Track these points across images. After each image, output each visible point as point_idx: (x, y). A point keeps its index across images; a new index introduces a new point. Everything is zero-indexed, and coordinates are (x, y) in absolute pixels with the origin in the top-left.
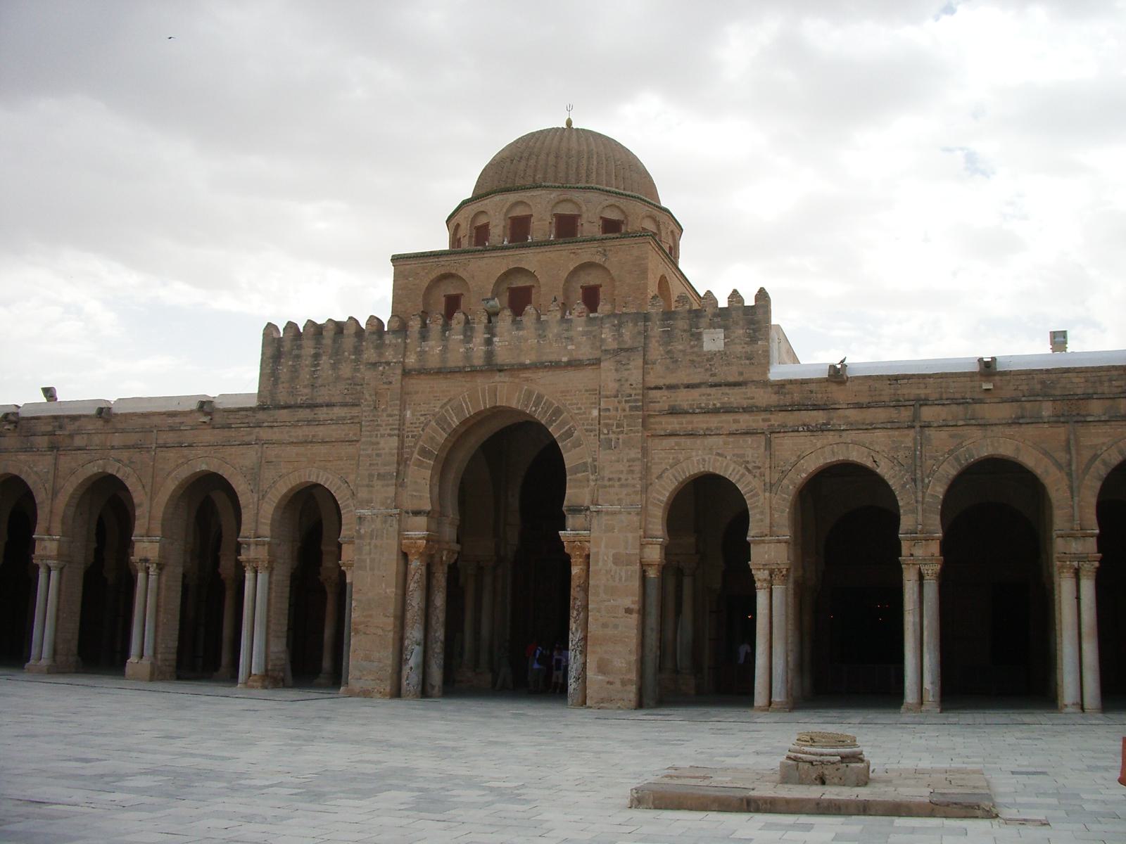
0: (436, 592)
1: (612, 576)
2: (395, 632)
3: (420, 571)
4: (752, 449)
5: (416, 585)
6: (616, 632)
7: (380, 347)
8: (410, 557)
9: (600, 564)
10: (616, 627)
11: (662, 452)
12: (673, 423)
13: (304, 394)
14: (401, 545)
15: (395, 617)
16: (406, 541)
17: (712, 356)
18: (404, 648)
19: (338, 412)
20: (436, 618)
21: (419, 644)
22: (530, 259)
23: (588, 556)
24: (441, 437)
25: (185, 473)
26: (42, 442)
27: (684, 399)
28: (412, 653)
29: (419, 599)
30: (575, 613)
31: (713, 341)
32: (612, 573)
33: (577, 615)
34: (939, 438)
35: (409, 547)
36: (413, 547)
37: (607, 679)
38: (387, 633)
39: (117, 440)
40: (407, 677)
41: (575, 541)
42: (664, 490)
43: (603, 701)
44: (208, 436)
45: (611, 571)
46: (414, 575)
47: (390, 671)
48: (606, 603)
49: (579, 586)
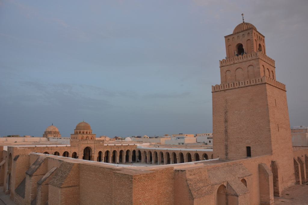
4: (103, 149)
7: (80, 142)
11: (98, 149)
12: (99, 148)
13: (74, 145)
17: (101, 144)
19: (77, 147)
22: (88, 135)
23: (94, 157)
24: (84, 148)
25: (64, 151)
26: (50, 149)
27: (99, 146)
31: (101, 143)
34: (112, 149)
39: (58, 149)
42: (98, 152)
44: (66, 148)
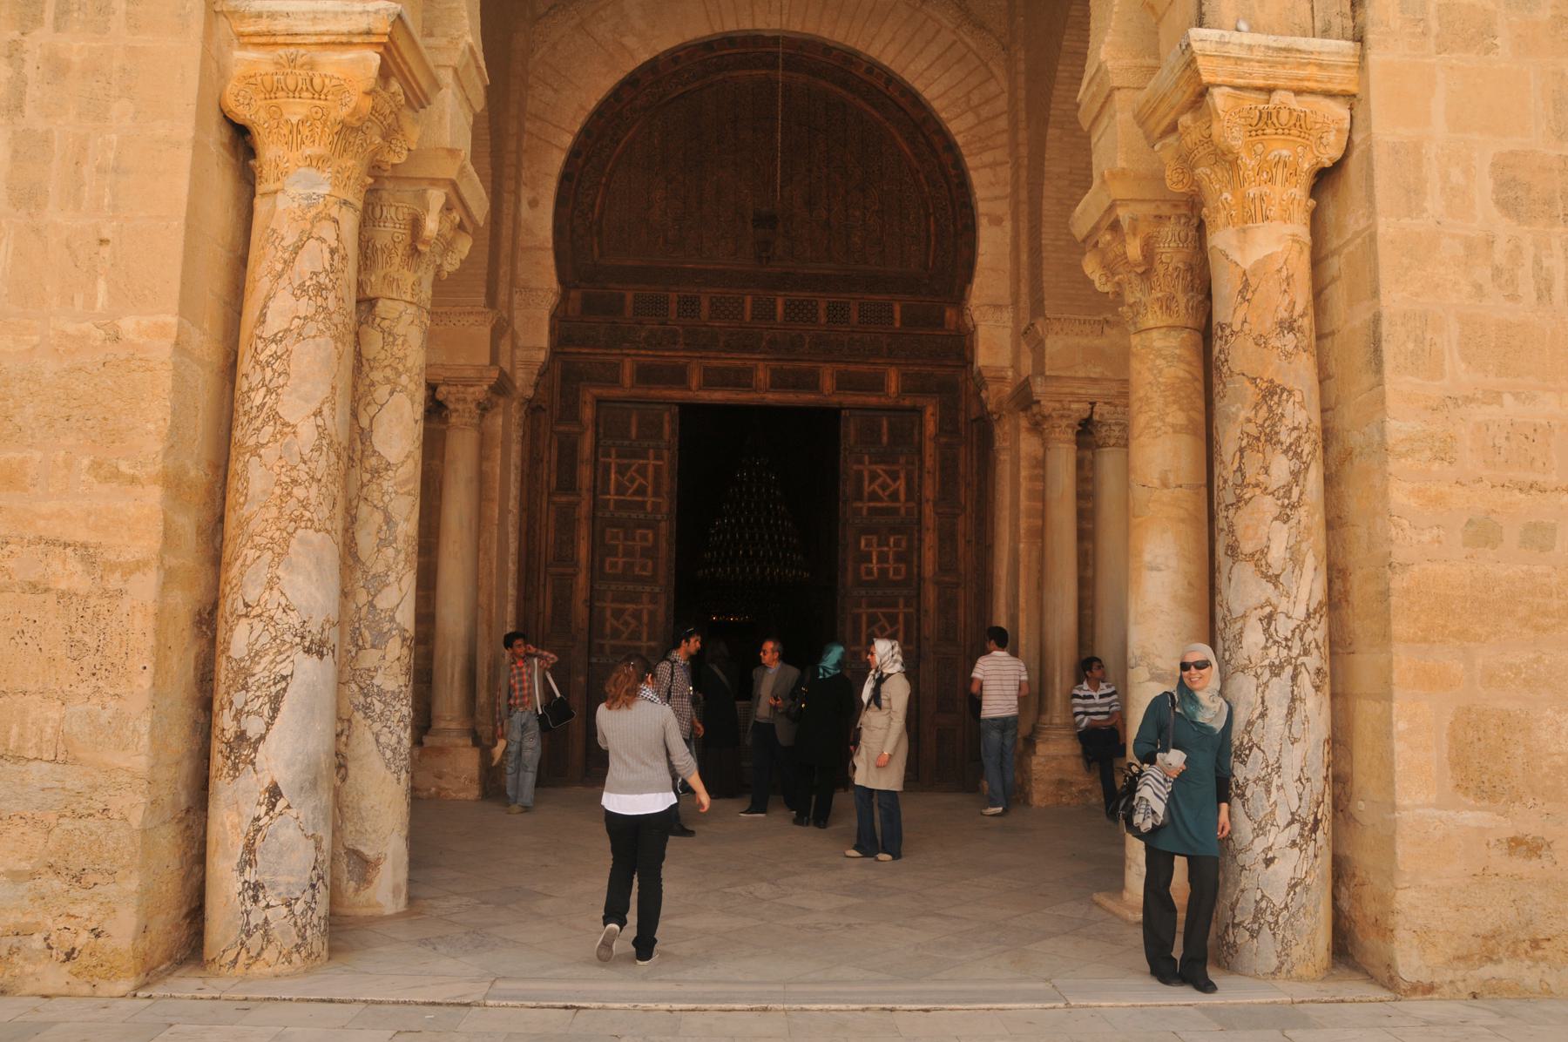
0: (382, 392)
1: (1497, 272)
2: (169, 578)
3: (327, 231)
5: (305, 307)
6: (1538, 569)
8: (270, 151)
9: (1434, 204)
10: (1538, 536)
14: (223, 74)
15: (173, 483)
16: (252, 55)
18: (223, 672)
20: (378, 517)
21: (316, 649)
28: (276, 702)
29: (323, 391)
30: (1281, 467)
32: (1499, 257)
33: (1295, 475)
35: (271, 92)
36: (295, 92)
37: (1508, 828)
38: (115, 581)
40: (250, 848)
41: (1270, 90)
43: (1489, 947)
45: (1490, 243)
46: (297, 249)
47: (136, 818)
48: (1480, 413)
49: (1288, 326)
